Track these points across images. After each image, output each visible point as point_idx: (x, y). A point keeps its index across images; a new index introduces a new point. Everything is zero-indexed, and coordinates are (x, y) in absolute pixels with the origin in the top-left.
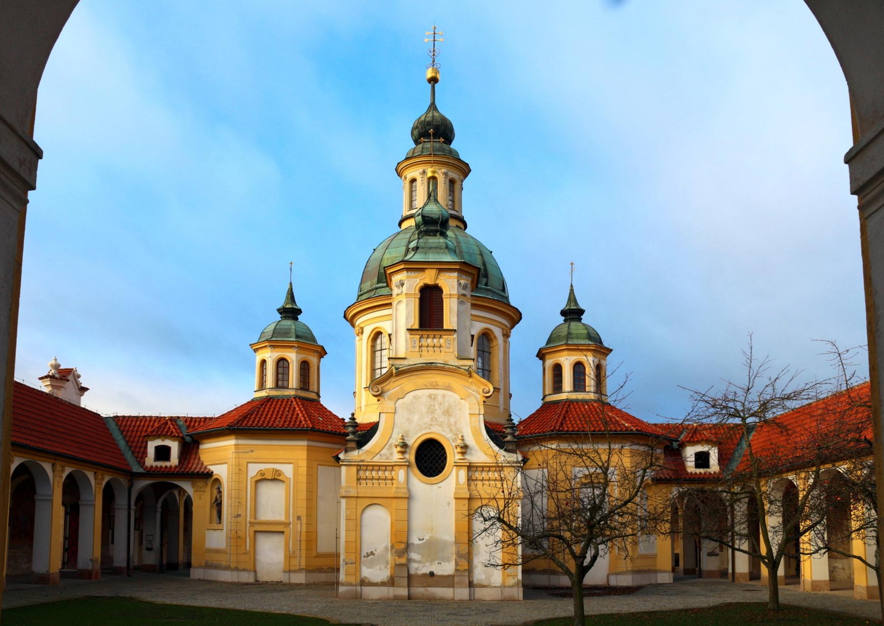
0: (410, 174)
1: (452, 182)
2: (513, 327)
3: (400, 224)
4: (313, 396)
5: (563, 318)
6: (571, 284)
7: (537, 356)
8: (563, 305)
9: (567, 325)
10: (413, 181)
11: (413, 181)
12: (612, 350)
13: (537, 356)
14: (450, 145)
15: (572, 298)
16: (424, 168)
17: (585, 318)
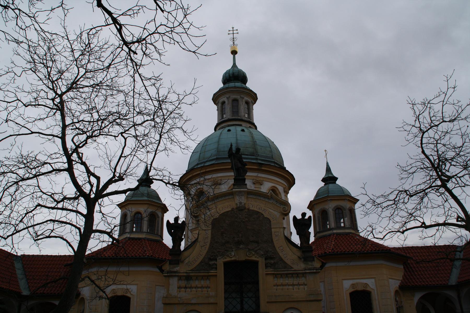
0: (221, 100)
1: (247, 103)
2: (290, 189)
3: (215, 129)
4: (159, 238)
5: (324, 183)
6: (327, 161)
7: (307, 208)
8: (323, 174)
10: (223, 103)
11: (223, 103)
12: (359, 200)
13: (307, 208)
14: (245, 84)
15: (328, 170)
16: (230, 95)
17: (337, 182)
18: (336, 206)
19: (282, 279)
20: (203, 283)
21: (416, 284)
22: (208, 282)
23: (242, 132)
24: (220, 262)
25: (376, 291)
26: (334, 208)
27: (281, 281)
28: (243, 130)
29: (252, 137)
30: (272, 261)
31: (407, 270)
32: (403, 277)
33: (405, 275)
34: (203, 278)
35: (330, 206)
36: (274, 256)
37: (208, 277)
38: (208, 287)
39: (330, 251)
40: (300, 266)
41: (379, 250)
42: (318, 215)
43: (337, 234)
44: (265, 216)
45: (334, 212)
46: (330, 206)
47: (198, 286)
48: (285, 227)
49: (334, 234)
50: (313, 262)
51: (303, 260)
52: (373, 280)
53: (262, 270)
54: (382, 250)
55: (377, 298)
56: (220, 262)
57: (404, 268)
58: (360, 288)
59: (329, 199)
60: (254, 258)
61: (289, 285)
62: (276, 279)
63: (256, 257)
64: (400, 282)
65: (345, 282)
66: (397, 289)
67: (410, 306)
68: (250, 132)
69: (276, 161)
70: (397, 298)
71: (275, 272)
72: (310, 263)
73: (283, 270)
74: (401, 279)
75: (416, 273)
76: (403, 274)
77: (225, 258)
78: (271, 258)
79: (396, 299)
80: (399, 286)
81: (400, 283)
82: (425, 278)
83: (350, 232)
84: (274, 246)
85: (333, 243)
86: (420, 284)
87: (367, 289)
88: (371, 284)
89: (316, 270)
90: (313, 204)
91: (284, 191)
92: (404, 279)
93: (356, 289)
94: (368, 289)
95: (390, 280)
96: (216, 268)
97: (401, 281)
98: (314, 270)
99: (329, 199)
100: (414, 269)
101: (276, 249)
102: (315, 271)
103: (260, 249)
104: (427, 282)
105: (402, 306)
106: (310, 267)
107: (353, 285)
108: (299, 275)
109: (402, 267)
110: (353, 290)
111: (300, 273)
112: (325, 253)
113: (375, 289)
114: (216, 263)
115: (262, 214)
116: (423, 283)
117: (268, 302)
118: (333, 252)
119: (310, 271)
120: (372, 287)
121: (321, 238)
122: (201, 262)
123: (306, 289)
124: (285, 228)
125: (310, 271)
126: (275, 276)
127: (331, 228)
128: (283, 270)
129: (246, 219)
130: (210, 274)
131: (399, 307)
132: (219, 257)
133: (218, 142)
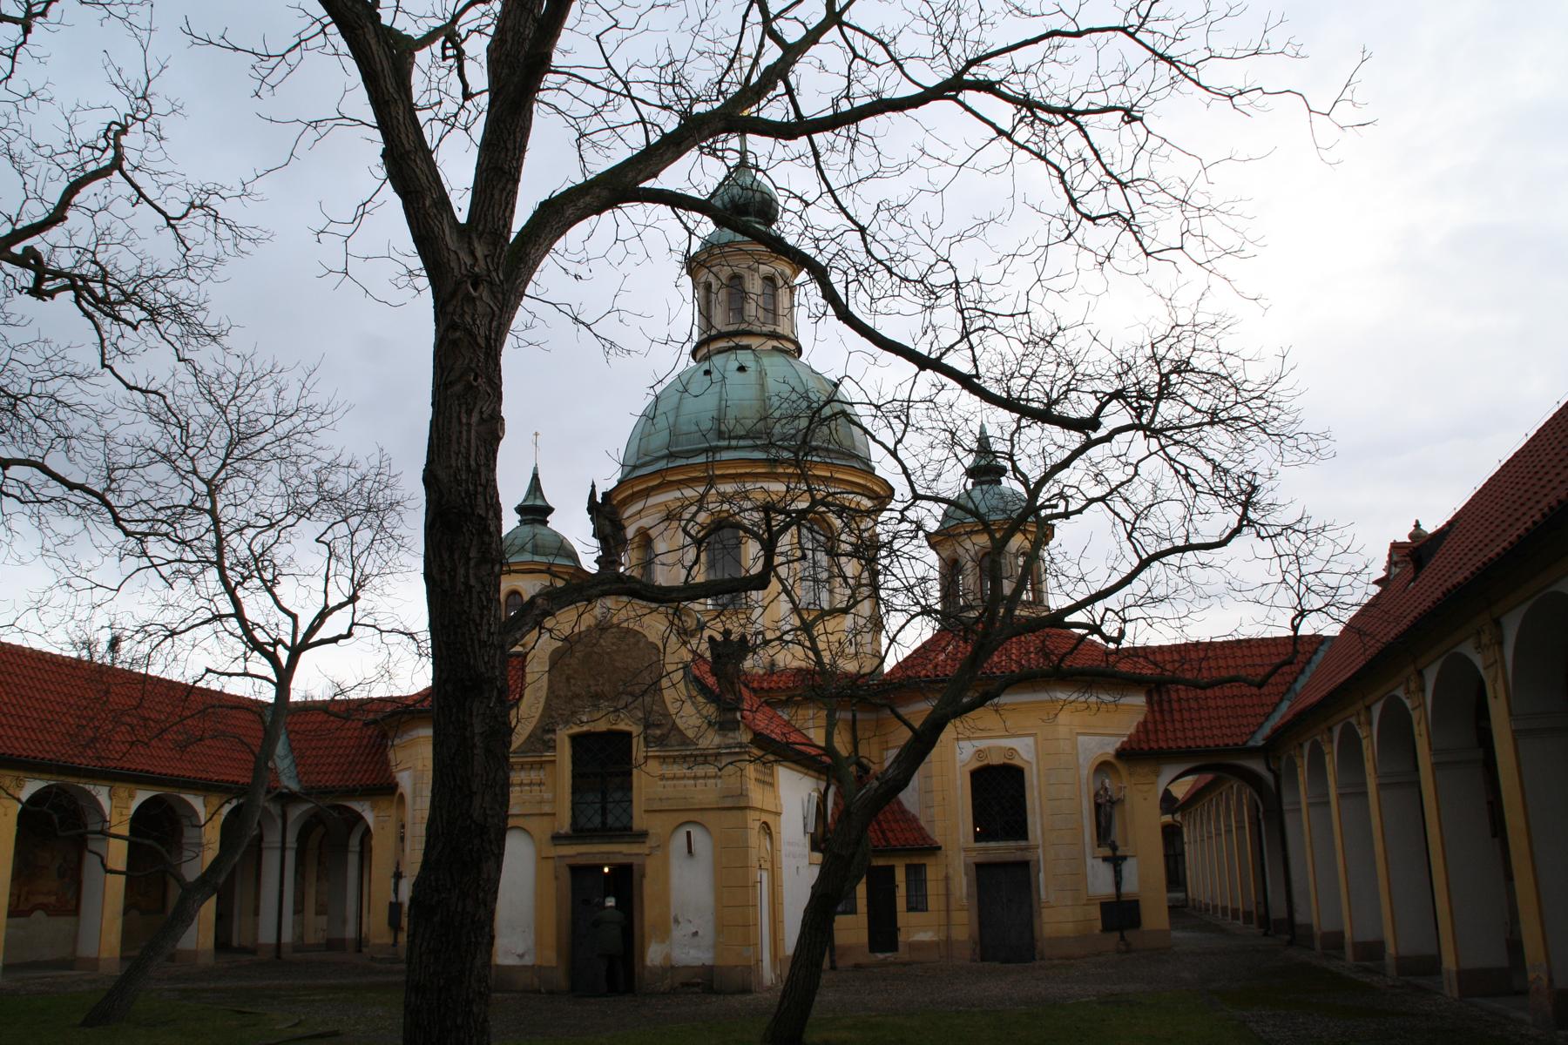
1: (769, 280)
19: (675, 767)
20: (534, 775)
22: (542, 773)
23: (742, 375)
24: (563, 737)
27: (677, 770)
28: (742, 369)
29: (762, 385)
30: (658, 732)
33: (1144, 723)
34: (532, 766)
36: (664, 722)
37: (541, 765)
38: (540, 784)
40: (711, 740)
44: (650, 640)
47: (525, 782)
50: (737, 732)
51: (717, 727)
52: (1030, 741)
53: (638, 749)
55: (1035, 782)
56: (563, 737)
58: (996, 760)
60: (622, 726)
61: (689, 778)
62: (664, 766)
63: (626, 724)
67: (1145, 799)
68: (760, 372)
70: (1107, 781)
71: (662, 754)
72: (731, 735)
73: (677, 748)
76: (1141, 718)
77: (571, 728)
78: (659, 726)
84: (664, 701)
88: (1024, 750)
89: (740, 747)
92: (1138, 731)
93: (985, 762)
94: (1016, 762)
96: (554, 748)
98: (735, 747)
101: (666, 707)
102: (737, 750)
103: (636, 708)
105: (1121, 801)
106: (731, 741)
107: (979, 753)
108: (709, 758)
110: (976, 765)
111: (711, 755)
114: (554, 737)
115: (645, 636)
117: (646, 811)
119: (728, 751)
120: (1025, 757)
122: (530, 736)
123: (719, 786)
125: (728, 751)
126: (663, 760)
128: (677, 748)
129: (614, 648)
130: (544, 759)
132: (561, 726)
133: (678, 408)
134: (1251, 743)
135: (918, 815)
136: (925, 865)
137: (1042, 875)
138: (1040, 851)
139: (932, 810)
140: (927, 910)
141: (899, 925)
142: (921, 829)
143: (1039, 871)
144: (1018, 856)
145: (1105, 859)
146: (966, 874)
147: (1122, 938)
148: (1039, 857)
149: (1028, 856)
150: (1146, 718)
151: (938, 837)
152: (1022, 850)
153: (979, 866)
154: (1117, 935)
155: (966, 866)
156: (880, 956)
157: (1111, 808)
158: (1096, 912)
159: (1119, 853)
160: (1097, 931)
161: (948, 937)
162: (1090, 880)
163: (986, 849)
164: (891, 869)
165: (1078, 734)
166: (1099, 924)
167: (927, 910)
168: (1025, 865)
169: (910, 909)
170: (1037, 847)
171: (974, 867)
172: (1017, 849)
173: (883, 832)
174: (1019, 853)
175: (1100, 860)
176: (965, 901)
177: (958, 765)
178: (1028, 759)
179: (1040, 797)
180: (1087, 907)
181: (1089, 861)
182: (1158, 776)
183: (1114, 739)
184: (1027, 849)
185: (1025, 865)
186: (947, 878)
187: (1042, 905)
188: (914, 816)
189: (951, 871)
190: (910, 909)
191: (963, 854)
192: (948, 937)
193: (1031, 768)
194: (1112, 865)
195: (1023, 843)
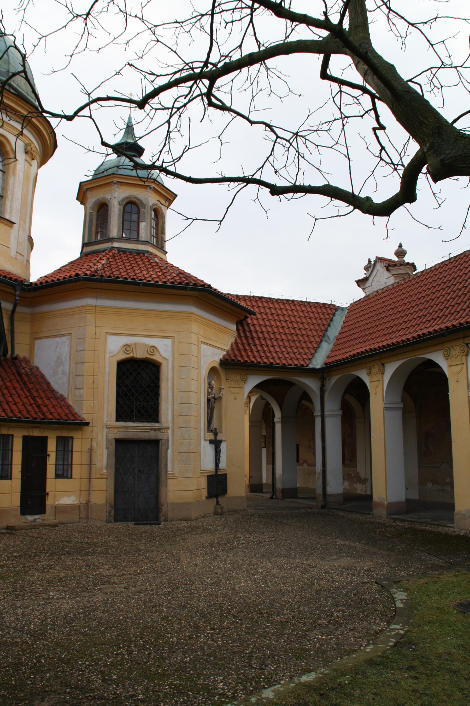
6: (130, 115)
9: (119, 158)
18: (127, 198)
21: (253, 359)
25: (170, 364)
26: (123, 200)
31: (242, 335)
32: (232, 345)
33: (236, 343)
35: (116, 195)
39: (88, 272)
41: (187, 284)
42: (91, 211)
43: (119, 251)
45: (122, 208)
46: (116, 195)
48: (13, 221)
49: (113, 248)
52: (168, 342)
54: (195, 284)
55: (170, 376)
57: (238, 329)
58: (140, 354)
59: (115, 180)
64: (225, 353)
65: (110, 338)
66: (217, 365)
69: (18, 85)
74: (228, 348)
75: (257, 342)
76: (233, 340)
79: (209, 384)
80: (221, 360)
81: (224, 356)
82: (270, 352)
83: (146, 249)
85: (103, 262)
86: (259, 360)
87: (154, 357)
90: (85, 188)
91: (25, 150)
92: (232, 349)
93: (131, 355)
94: (156, 358)
95: (204, 346)
97: (228, 352)
99: (115, 180)
100: (255, 335)
104: (273, 358)
105: (220, 398)
109: (234, 327)
110: (124, 356)
112: (77, 275)
113: (170, 359)
116: (265, 360)
118: (94, 275)
120: (164, 355)
121: (87, 255)
124: (14, 223)
127: (111, 236)
131: (214, 398)
134: (311, 366)
135: (65, 395)
136: (72, 438)
137: (169, 452)
138: (170, 432)
139: (82, 391)
140: (71, 478)
141: (48, 490)
142: (69, 407)
143: (168, 448)
144: (152, 435)
145: (211, 442)
146: (107, 448)
147: (217, 502)
148: (168, 437)
149: (160, 435)
150: (236, 340)
151: (86, 417)
152: (155, 430)
153: (118, 442)
154: (215, 500)
155: (108, 440)
156: (30, 518)
157: (214, 403)
158: (204, 483)
159: (218, 438)
160: (204, 498)
161: (88, 502)
162: (202, 457)
163: (127, 428)
164: (44, 440)
165: (203, 342)
166: (205, 493)
167: (71, 478)
168: (156, 443)
169: (57, 476)
170: (167, 429)
171: (114, 441)
172: (151, 430)
173: (38, 406)
174: (152, 432)
175: (208, 442)
176: (105, 471)
177: (108, 355)
178: (166, 357)
179: (173, 388)
180: (199, 479)
181: (202, 441)
182: (245, 383)
183: (219, 351)
184: (159, 429)
185: (156, 443)
186: (91, 450)
187: (168, 476)
188: (61, 395)
189: (94, 444)
190: (57, 476)
191: (106, 430)
192: (88, 502)
193: (168, 364)
194: (214, 446)
195: (157, 425)
